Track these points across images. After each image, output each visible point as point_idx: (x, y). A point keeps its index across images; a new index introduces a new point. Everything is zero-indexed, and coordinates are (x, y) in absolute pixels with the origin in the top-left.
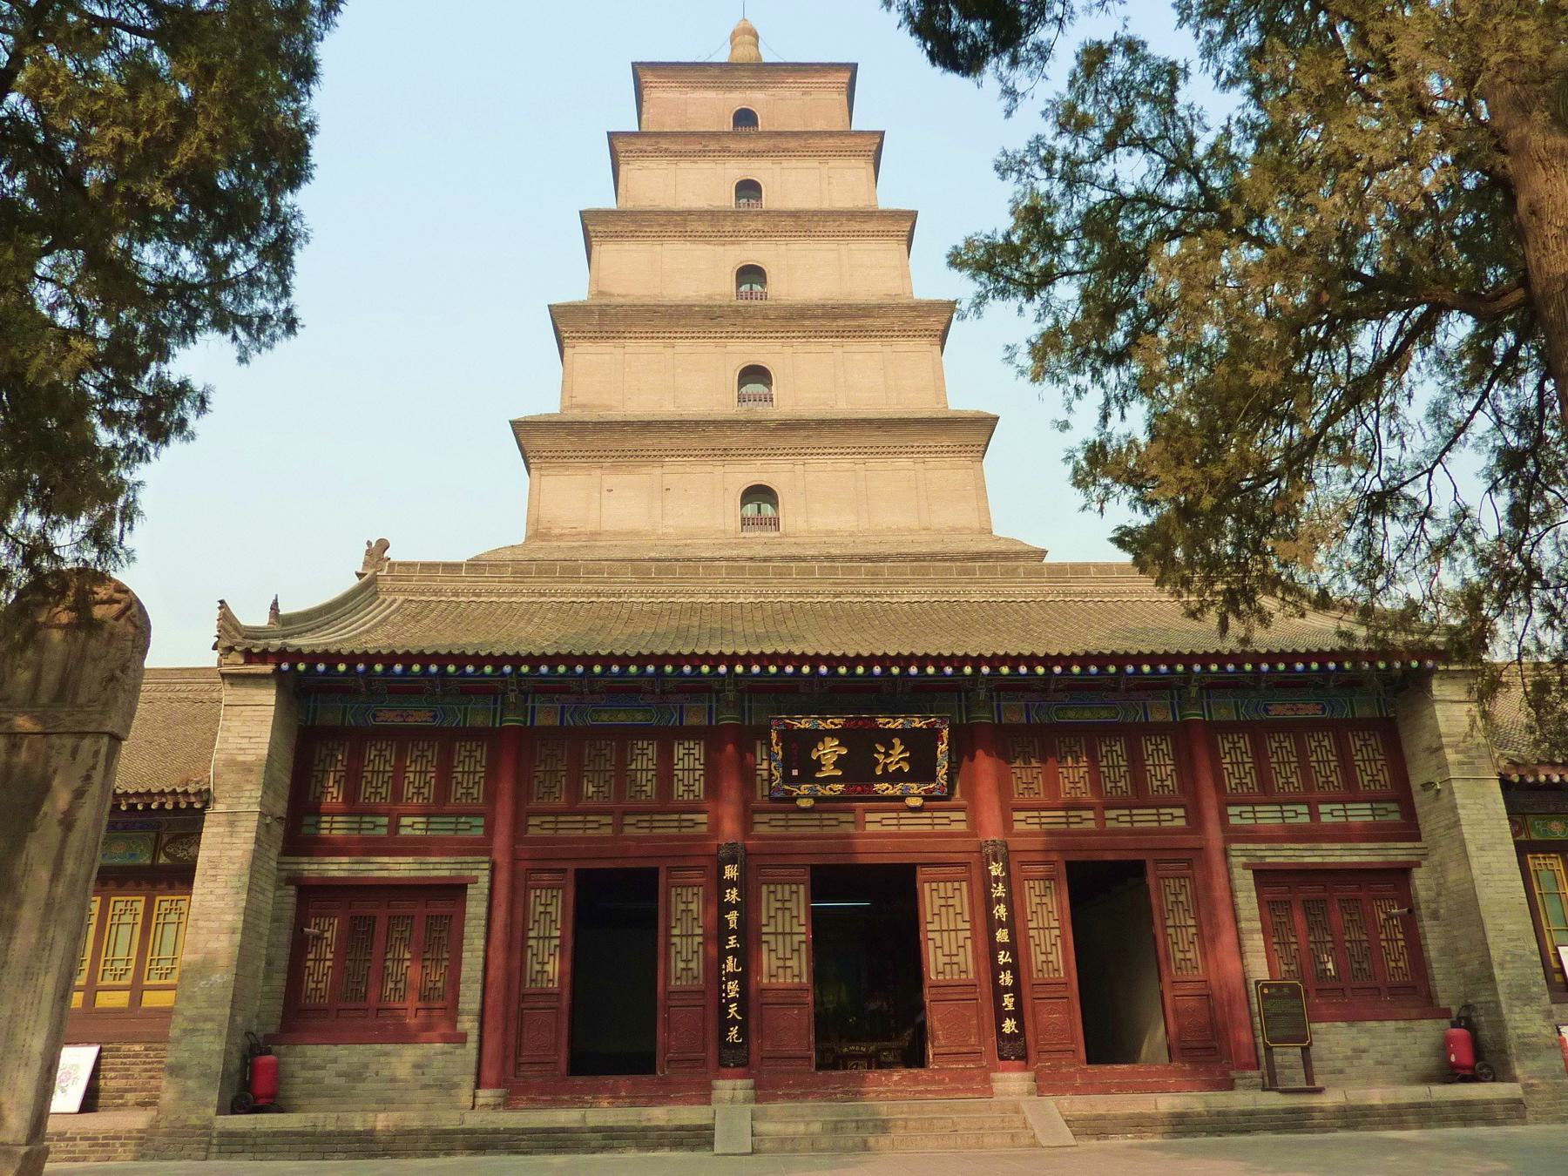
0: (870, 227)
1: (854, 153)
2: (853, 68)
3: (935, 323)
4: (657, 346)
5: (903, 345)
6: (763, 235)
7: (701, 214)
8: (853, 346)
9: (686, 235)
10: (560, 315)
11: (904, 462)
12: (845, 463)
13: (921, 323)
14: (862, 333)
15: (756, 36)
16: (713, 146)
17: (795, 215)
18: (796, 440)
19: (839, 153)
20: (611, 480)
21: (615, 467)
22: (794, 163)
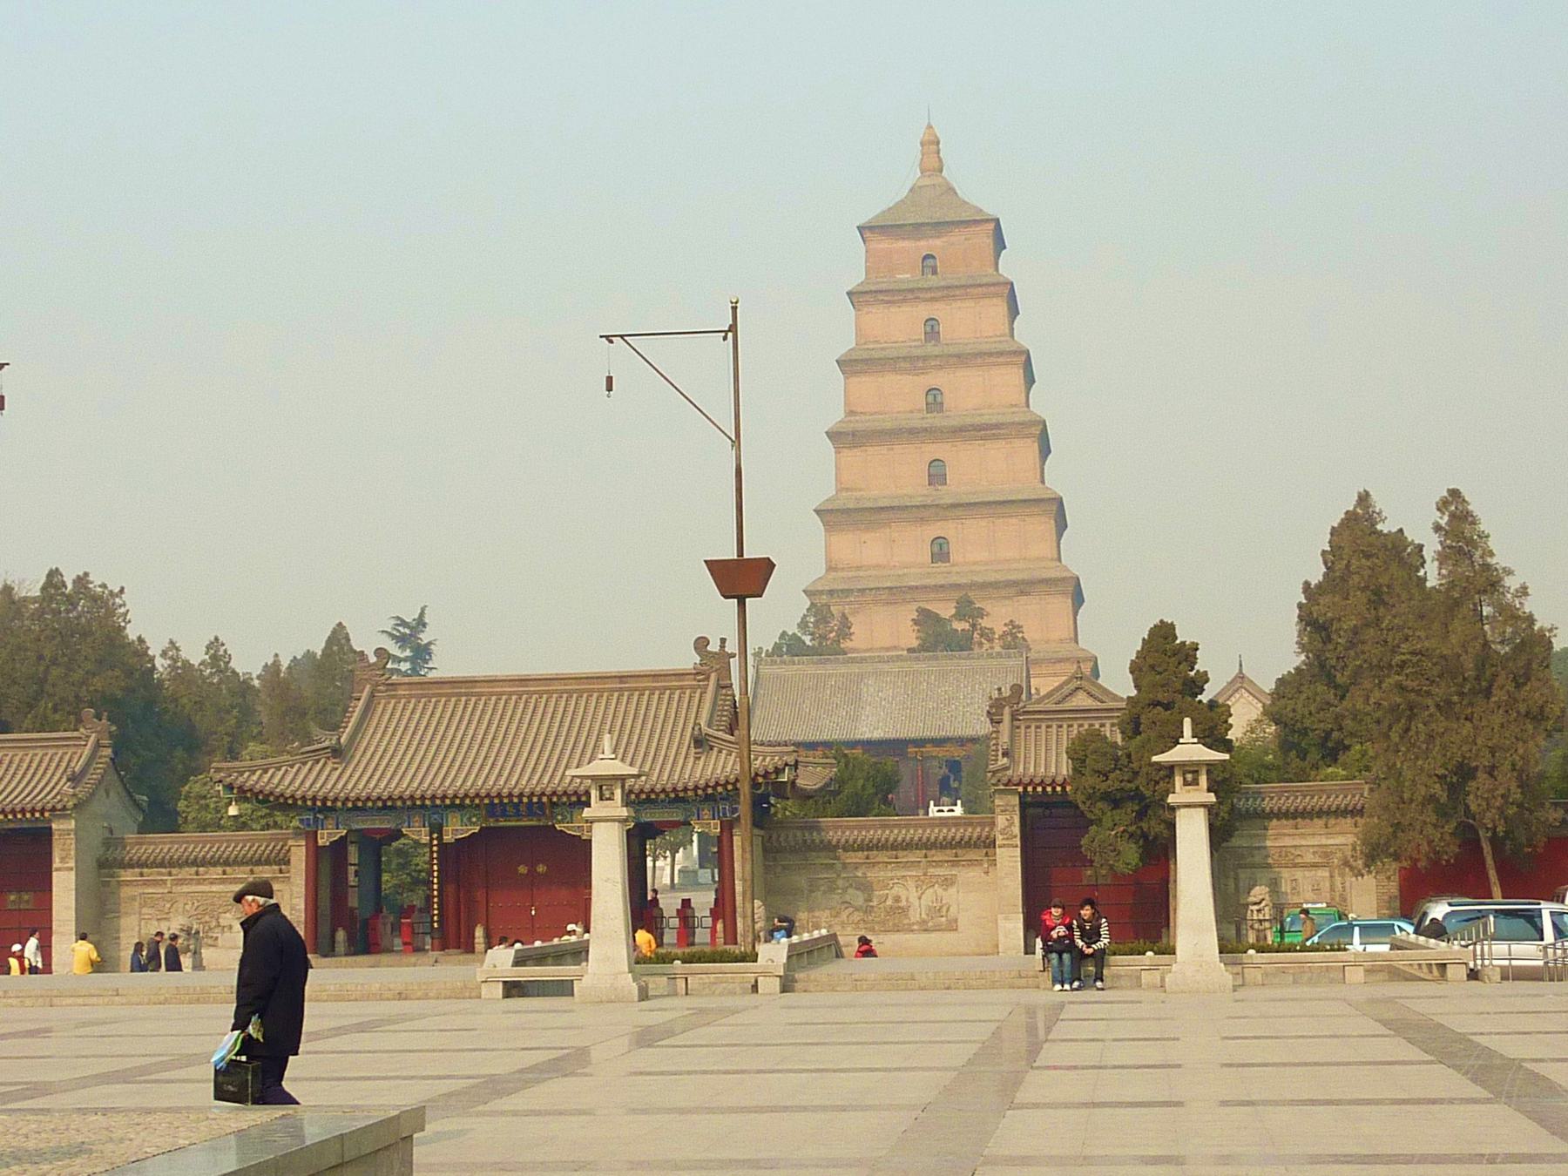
0: (1001, 360)
1: (996, 295)
2: (997, 221)
3: (1036, 430)
4: (884, 450)
5: (1017, 443)
6: (941, 367)
7: (904, 358)
8: (989, 444)
9: (895, 371)
10: (833, 436)
11: (1014, 521)
12: (983, 523)
13: (1026, 431)
14: (996, 437)
15: (938, 143)
16: (910, 296)
17: (958, 356)
18: (959, 512)
19: (984, 296)
20: (866, 536)
21: (867, 530)
22: (959, 304)
